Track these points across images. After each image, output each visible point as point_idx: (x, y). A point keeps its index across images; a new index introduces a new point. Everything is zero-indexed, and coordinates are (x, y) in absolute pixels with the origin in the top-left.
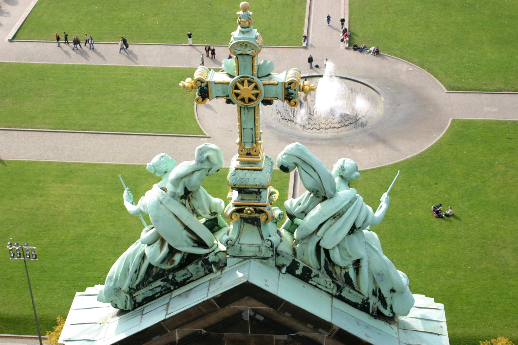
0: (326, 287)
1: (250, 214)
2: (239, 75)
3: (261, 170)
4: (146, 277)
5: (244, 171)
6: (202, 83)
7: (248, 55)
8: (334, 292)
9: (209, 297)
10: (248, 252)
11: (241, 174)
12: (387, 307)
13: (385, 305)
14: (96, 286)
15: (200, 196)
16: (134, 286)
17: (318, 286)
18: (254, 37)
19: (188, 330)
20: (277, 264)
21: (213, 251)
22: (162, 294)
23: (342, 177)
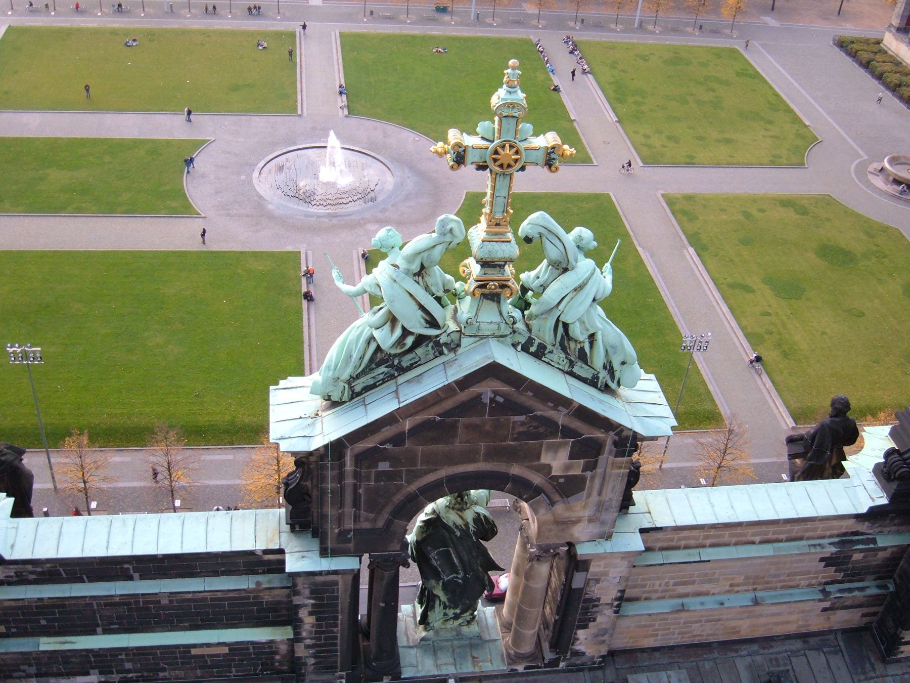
0: (559, 364)
7: (514, 117)
8: (566, 368)
9: (451, 380)
10: (486, 330)
17: (551, 362)
19: (419, 418)
21: (445, 331)
22: (384, 381)
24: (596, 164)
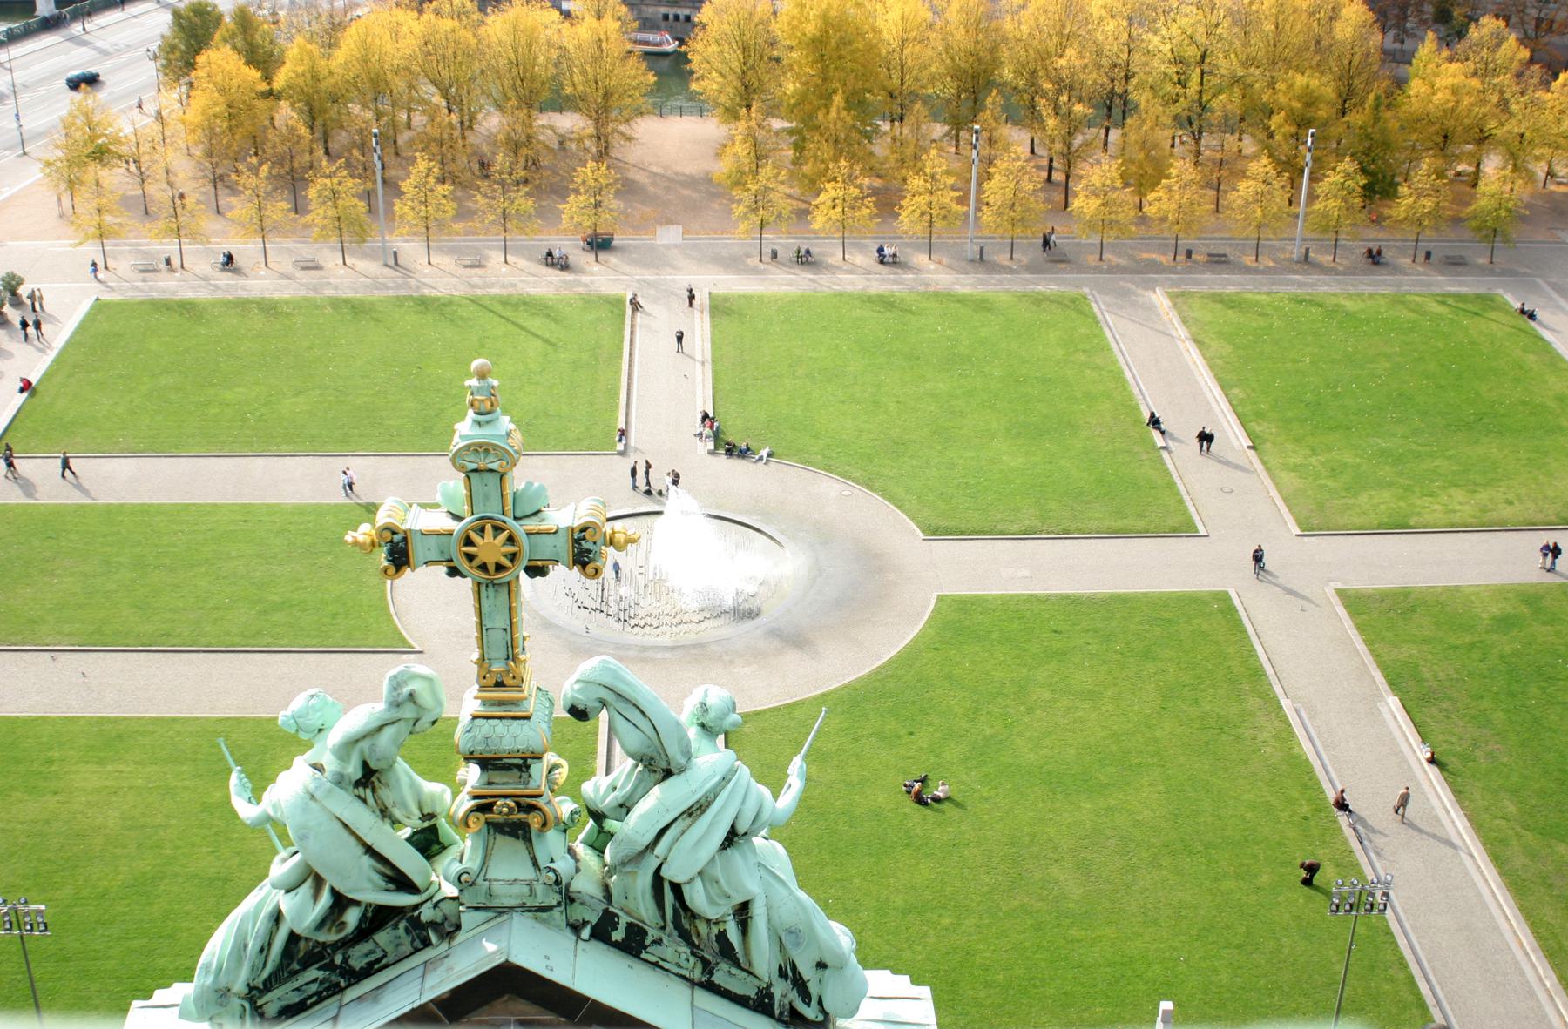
0: (679, 966)
1: (507, 814)
2: (473, 514)
3: (527, 718)
4: (285, 962)
5: (490, 721)
6: (394, 533)
7: (491, 471)
8: (697, 975)
9: (424, 1000)
10: (507, 896)
11: (485, 727)
12: (810, 1000)
13: (805, 996)
14: (176, 985)
15: (398, 780)
16: (259, 983)
17: (661, 963)
18: (504, 433)
20: (571, 921)
21: (431, 898)
22: (320, 998)
23: (703, 726)
24: (1202, 532)
